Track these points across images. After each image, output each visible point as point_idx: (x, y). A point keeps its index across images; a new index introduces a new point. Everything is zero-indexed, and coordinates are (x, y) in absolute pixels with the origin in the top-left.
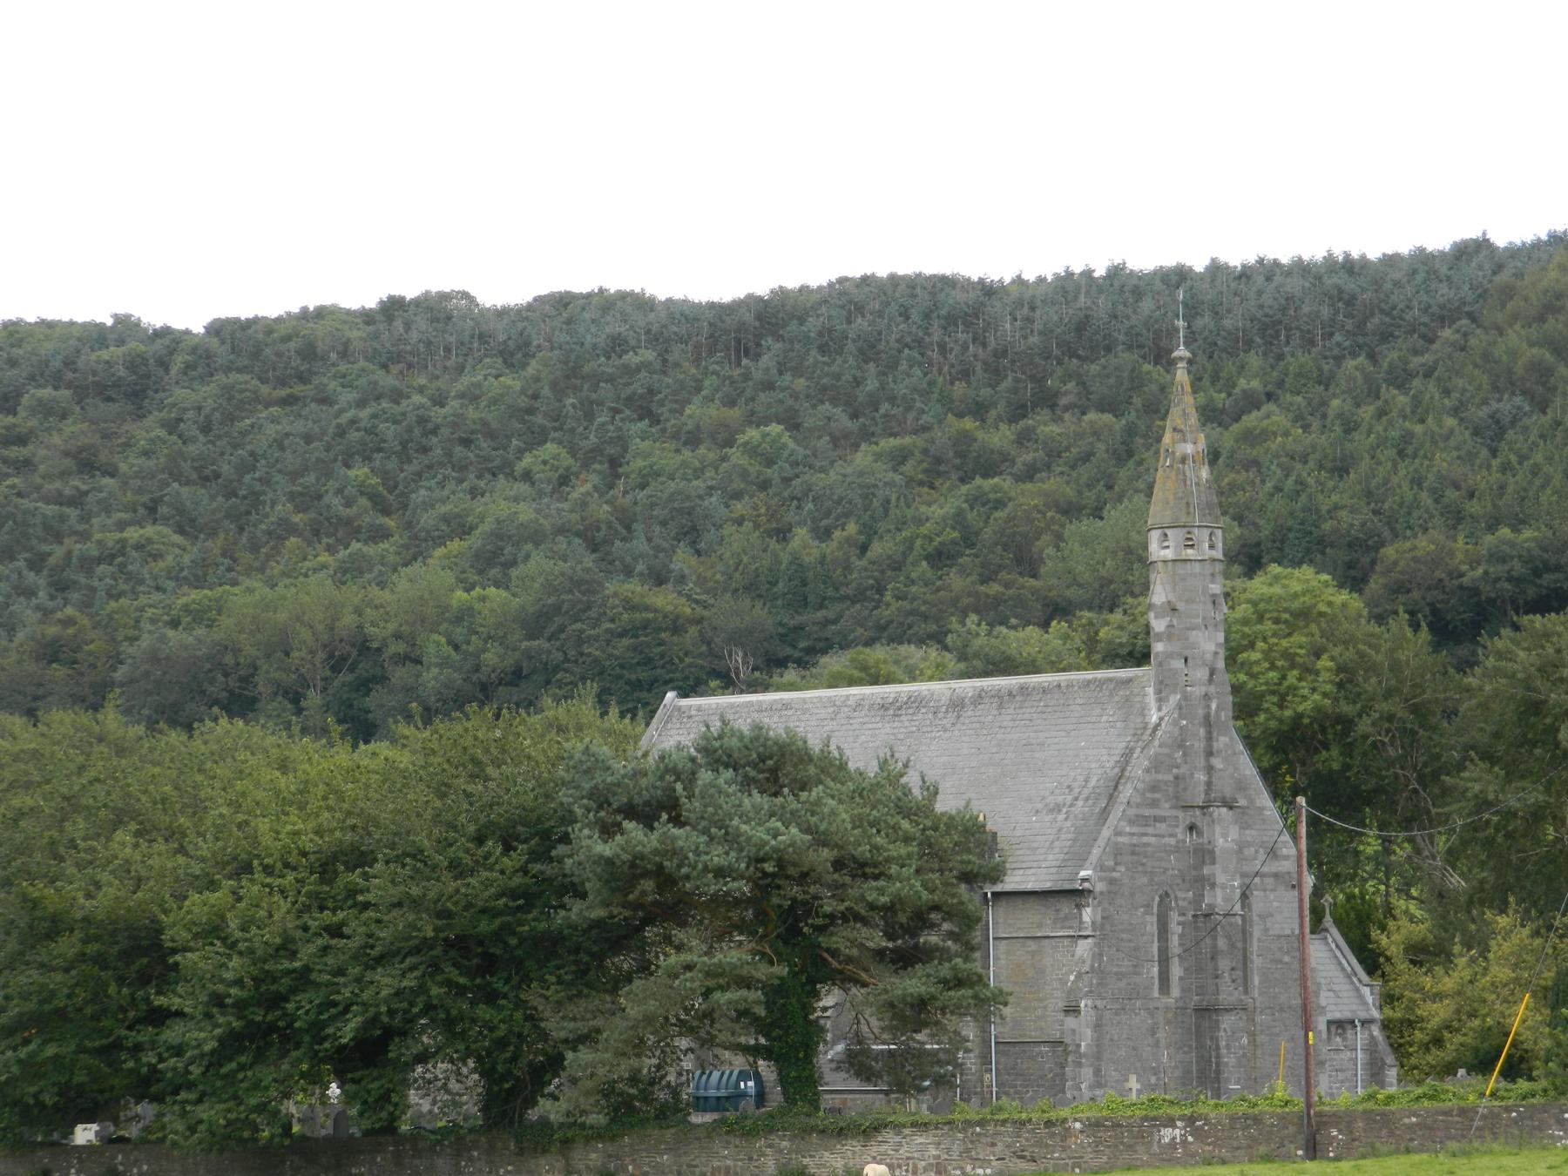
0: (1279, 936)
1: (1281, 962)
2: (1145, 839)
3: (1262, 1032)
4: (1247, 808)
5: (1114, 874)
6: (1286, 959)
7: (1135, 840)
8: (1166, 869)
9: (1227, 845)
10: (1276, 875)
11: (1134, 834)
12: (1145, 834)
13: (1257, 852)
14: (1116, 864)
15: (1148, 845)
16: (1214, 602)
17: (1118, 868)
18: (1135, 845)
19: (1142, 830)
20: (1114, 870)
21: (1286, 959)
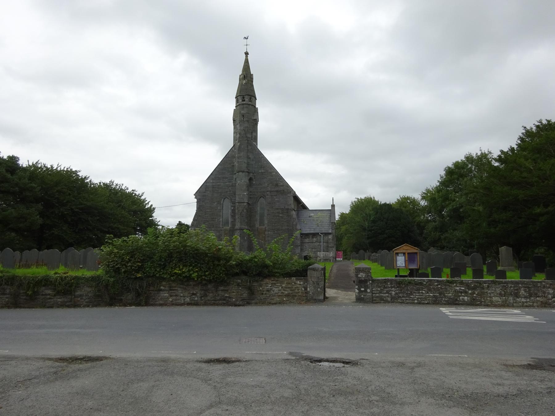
0: (277, 209)
1: (278, 216)
2: (218, 184)
3: (268, 237)
4: (265, 172)
5: (206, 194)
6: (281, 215)
7: (214, 184)
8: (227, 191)
9: (241, 183)
10: (277, 191)
11: (214, 182)
12: (219, 182)
13: (268, 185)
14: (206, 191)
15: (220, 185)
16: (243, 116)
17: (206, 192)
18: (214, 186)
19: (218, 181)
20: (205, 192)
21: (281, 215)
